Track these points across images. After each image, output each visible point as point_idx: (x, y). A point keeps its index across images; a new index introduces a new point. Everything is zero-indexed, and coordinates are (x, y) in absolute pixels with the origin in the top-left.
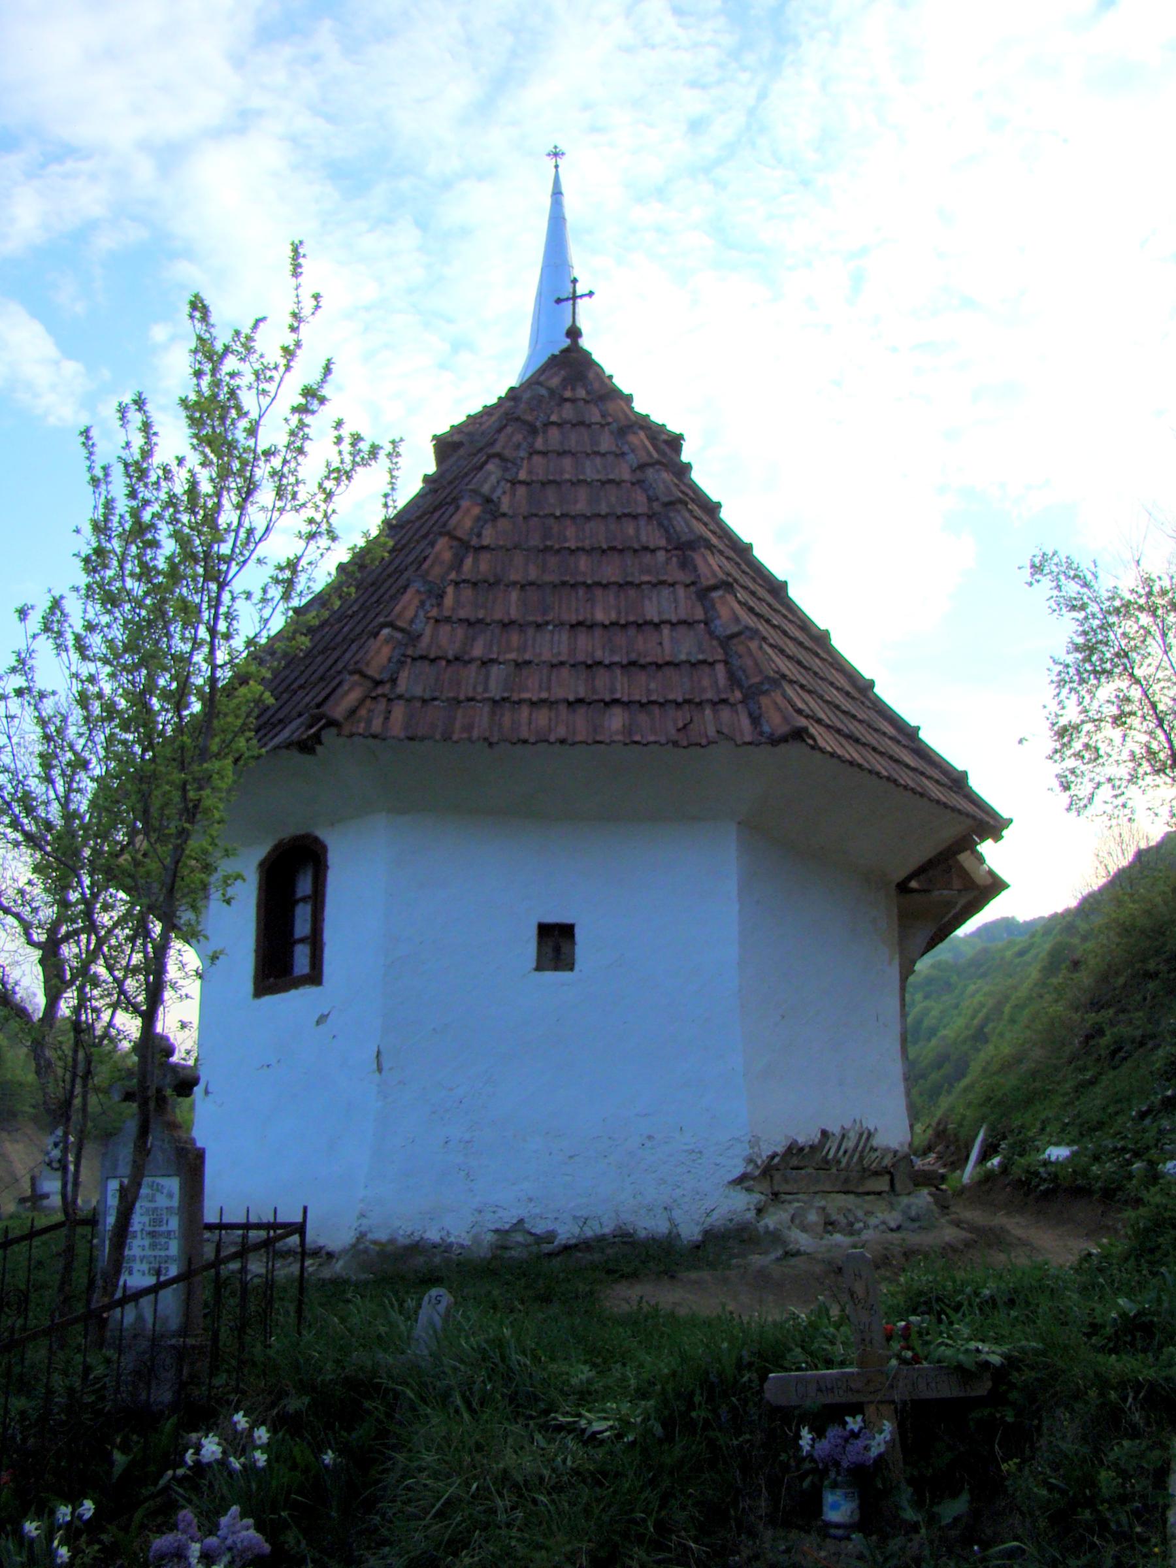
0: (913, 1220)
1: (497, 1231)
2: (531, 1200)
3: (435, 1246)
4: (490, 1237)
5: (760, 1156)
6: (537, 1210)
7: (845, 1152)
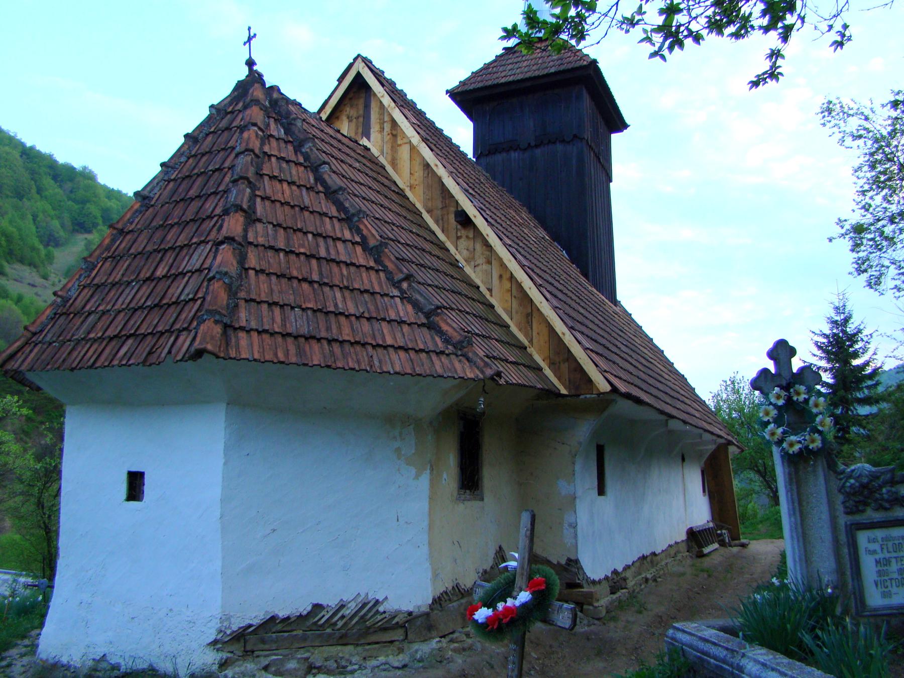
0: (421, 660)
1: (94, 660)
2: (111, 643)
3: (63, 666)
4: (91, 663)
5: (229, 627)
6: (113, 650)
7: (343, 617)
